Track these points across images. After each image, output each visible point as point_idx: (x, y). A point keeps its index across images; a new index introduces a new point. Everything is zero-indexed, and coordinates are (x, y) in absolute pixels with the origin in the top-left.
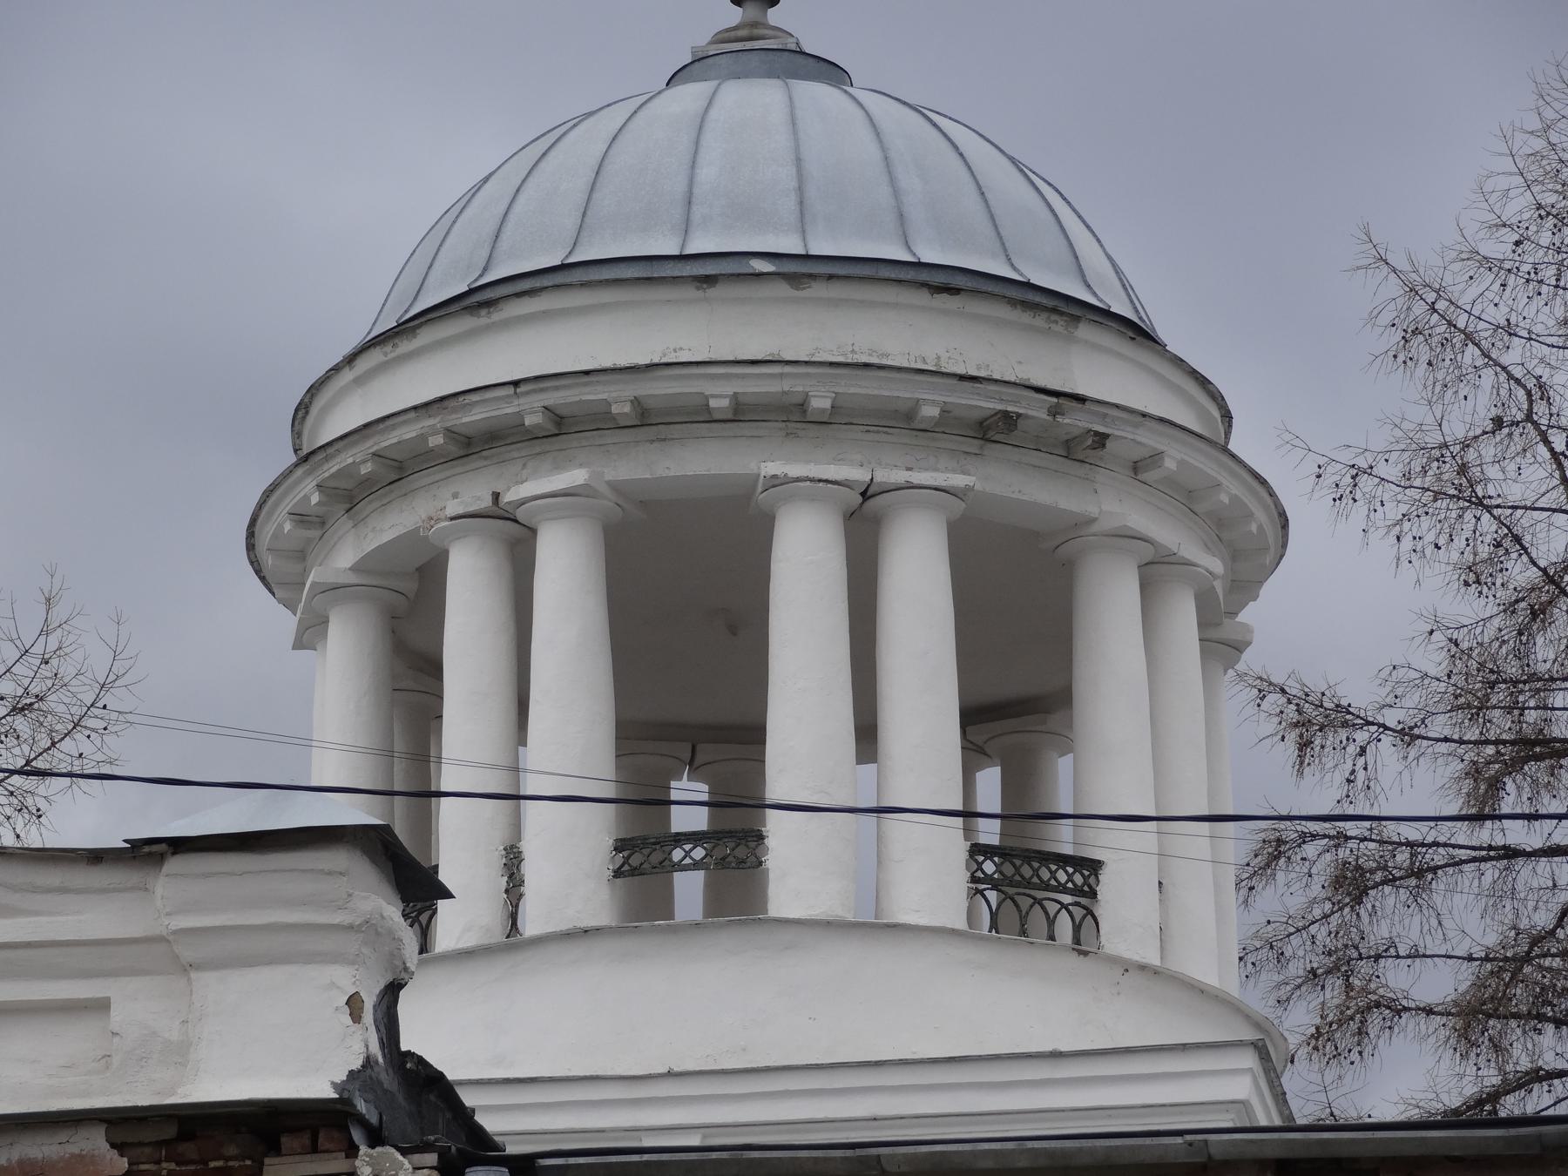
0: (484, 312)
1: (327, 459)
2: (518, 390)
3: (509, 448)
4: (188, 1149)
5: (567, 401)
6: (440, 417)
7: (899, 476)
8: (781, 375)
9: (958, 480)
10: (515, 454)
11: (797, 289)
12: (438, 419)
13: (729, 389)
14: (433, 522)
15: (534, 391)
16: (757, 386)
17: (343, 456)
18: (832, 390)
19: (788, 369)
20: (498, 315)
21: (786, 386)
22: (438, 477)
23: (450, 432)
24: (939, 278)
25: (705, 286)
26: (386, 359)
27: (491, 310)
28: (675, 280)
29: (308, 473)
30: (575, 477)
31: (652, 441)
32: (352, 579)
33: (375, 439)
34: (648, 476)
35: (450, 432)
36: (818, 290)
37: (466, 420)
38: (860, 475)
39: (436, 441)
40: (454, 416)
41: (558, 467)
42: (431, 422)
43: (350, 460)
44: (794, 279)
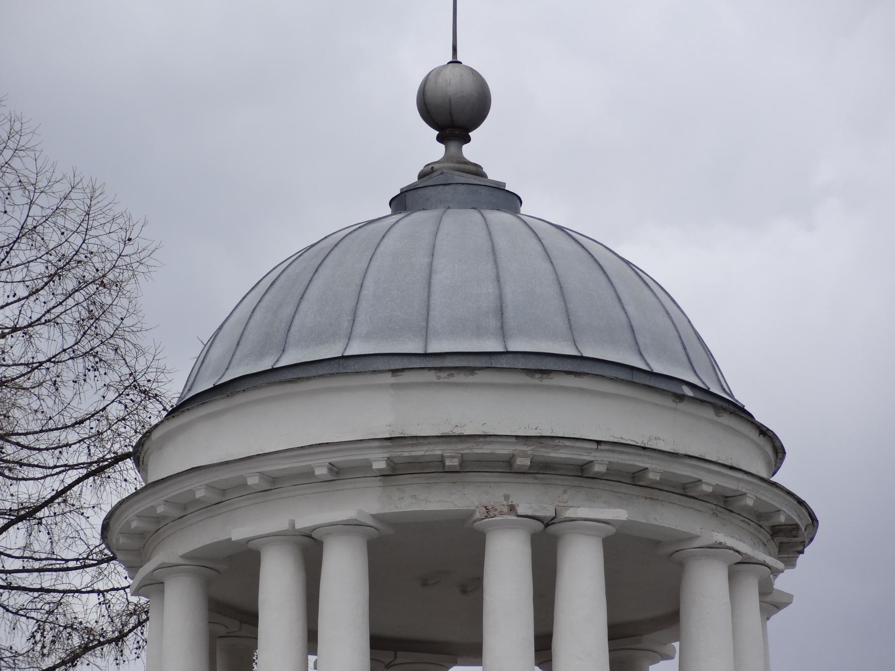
0: (538, 376)
1: (412, 445)
2: (599, 447)
3: (558, 477)
5: (627, 463)
6: (532, 447)
8: (740, 480)
10: (560, 482)
11: (717, 415)
12: (530, 448)
14: (496, 513)
15: (608, 450)
17: (431, 447)
18: (756, 495)
19: (745, 477)
20: (546, 381)
22: (490, 479)
25: (677, 401)
26: (438, 381)
27: (544, 376)
28: (663, 392)
29: (379, 447)
31: (646, 498)
32: (370, 522)
33: (470, 445)
34: (645, 522)
37: (552, 455)
40: (544, 450)
42: (524, 448)
43: (439, 452)
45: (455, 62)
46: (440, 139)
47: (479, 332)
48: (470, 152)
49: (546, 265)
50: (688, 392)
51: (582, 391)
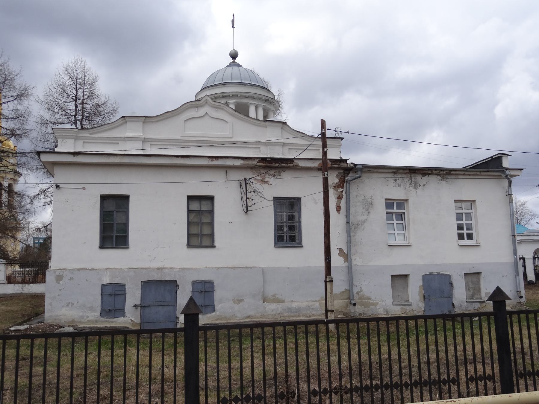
4: (335, 162)
7: (260, 104)
9: (264, 105)
13: (248, 95)
16: (251, 95)
20: (225, 86)
21: (253, 95)
23: (222, 96)
24: (263, 87)
30: (235, 101)
35: (222, 96)
36: (254, 87)
38: (257, 103)
39: (221, 96)
41: (232, 100)
44: (252, 86)
45: (234, 49)
46: (232, 59)
47: (220, 81)
48: (236, 61)
49: (247, 73)
50: (249, 84)
51: (230, 86)
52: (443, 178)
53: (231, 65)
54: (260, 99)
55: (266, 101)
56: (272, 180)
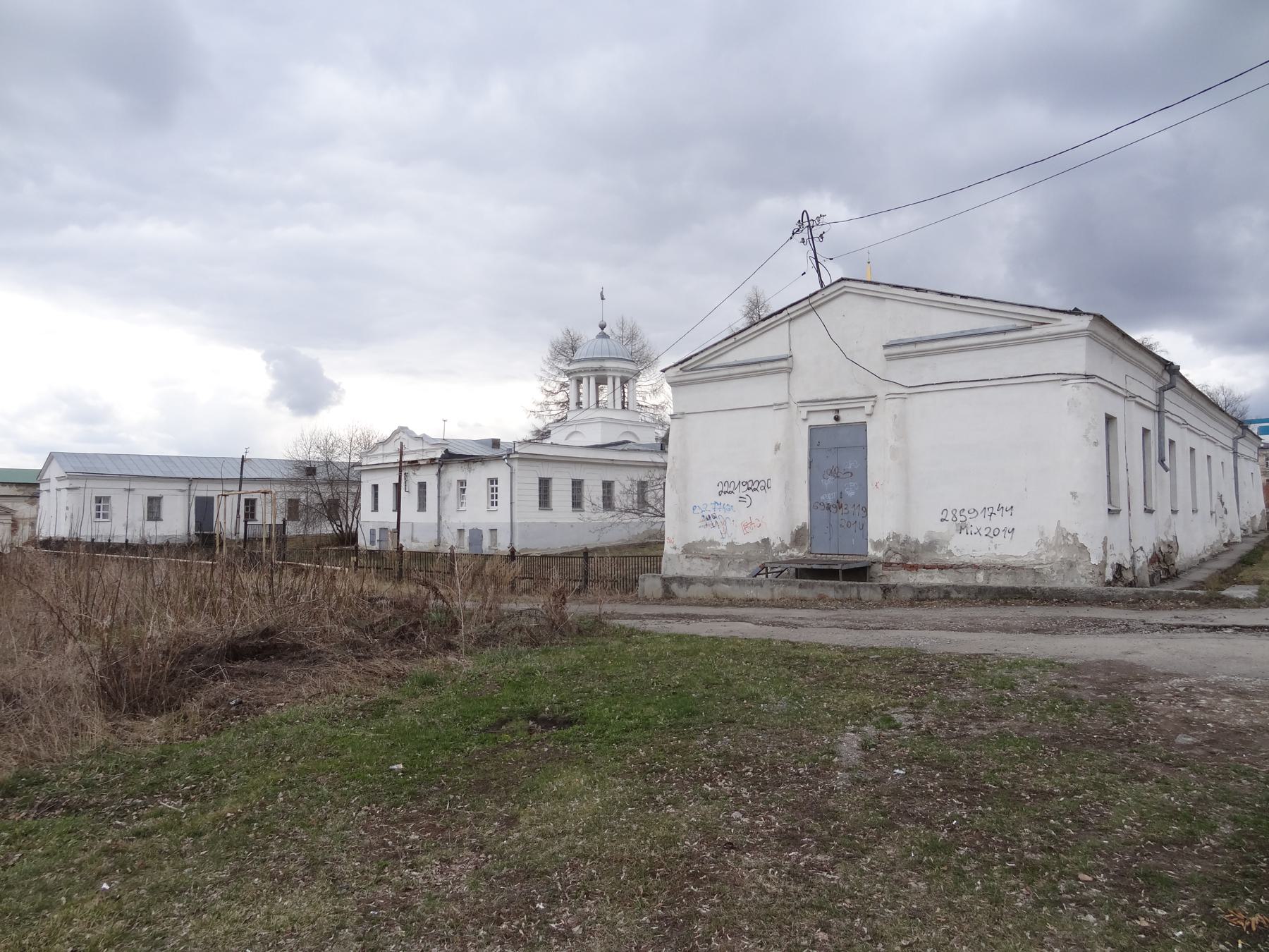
52: (483, 464)
53: (598, 337)
54: (588, 371)
55: (596, 370)
56: (417, 472)
